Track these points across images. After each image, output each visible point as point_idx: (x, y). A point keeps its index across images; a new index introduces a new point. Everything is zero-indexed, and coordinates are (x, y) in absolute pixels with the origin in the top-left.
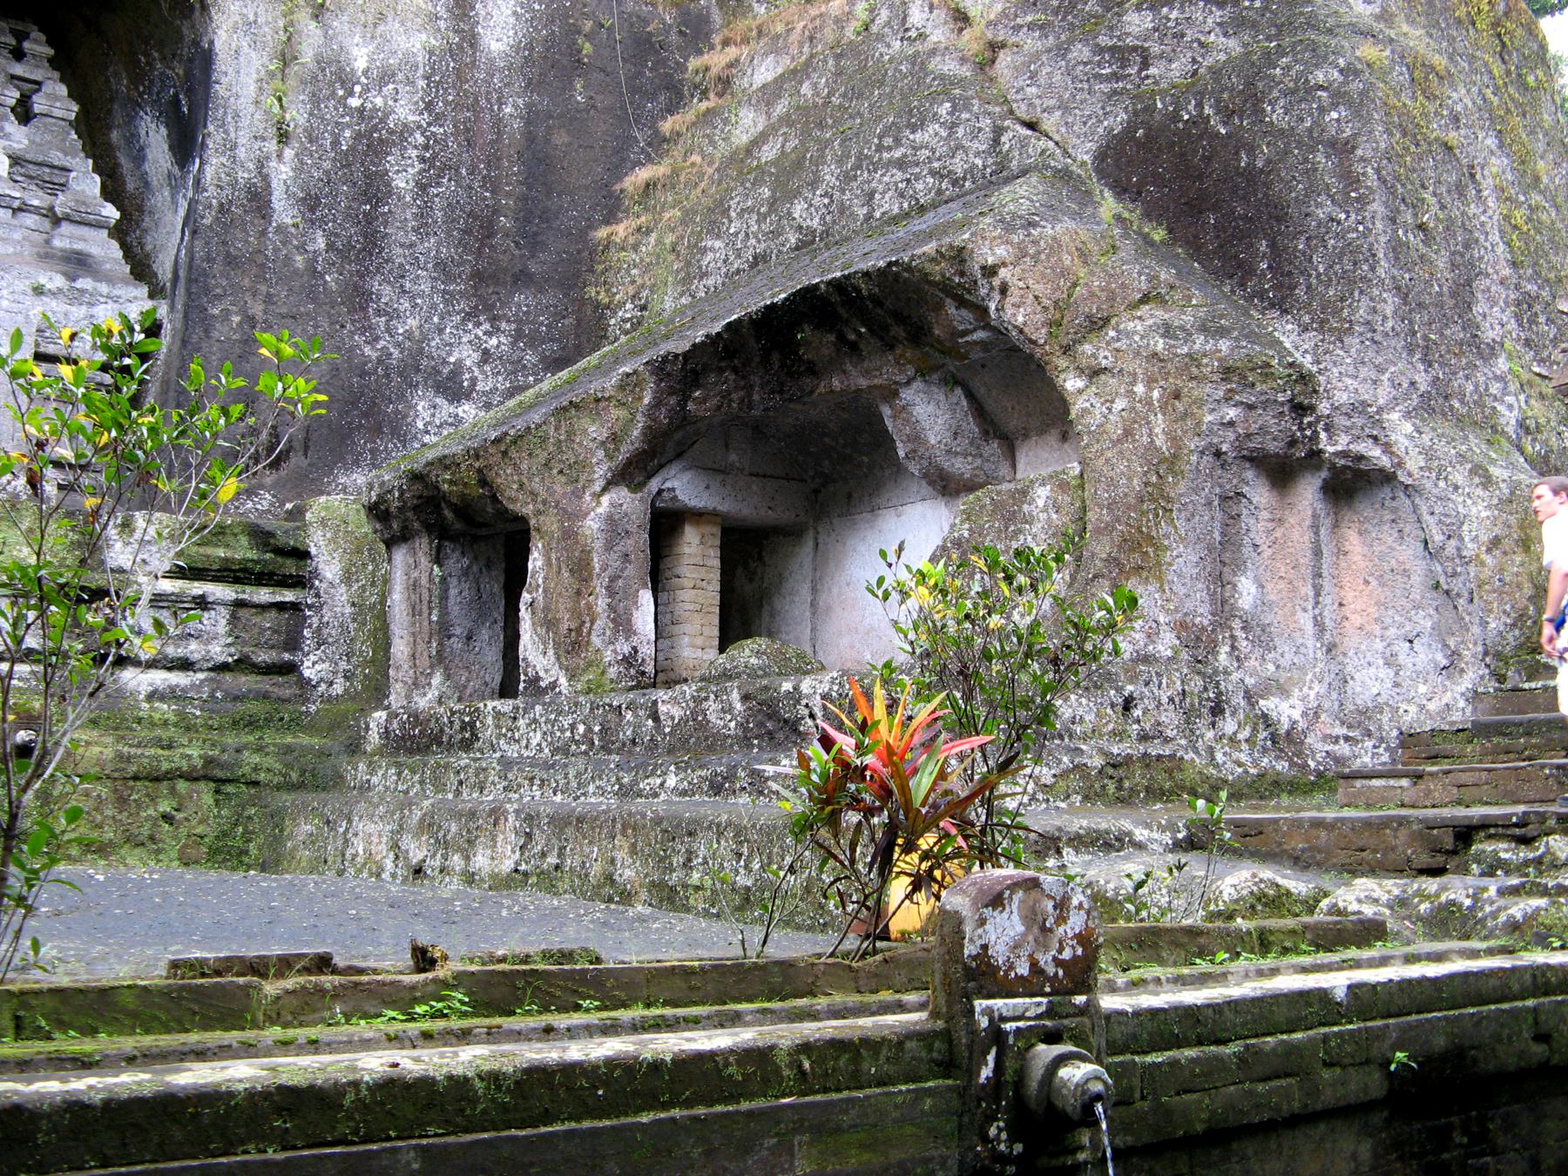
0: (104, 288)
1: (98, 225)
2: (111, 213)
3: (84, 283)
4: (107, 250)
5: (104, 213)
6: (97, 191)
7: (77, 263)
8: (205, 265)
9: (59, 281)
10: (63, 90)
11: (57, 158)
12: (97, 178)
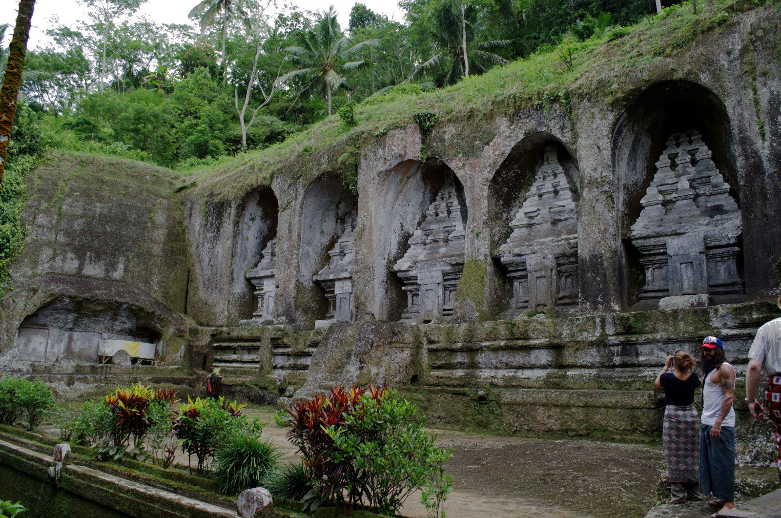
0: (725, 216)
1: (724, 193)
2: (727, 186)
3: (718, 217)
4: (727, 202)
5: (723, 187)
6: (722, 180)
7: (718, 210)
8: (745, 200)
9: (708, 219)
10: (706, 148)
11: (705, 174)
12: (721, 175)
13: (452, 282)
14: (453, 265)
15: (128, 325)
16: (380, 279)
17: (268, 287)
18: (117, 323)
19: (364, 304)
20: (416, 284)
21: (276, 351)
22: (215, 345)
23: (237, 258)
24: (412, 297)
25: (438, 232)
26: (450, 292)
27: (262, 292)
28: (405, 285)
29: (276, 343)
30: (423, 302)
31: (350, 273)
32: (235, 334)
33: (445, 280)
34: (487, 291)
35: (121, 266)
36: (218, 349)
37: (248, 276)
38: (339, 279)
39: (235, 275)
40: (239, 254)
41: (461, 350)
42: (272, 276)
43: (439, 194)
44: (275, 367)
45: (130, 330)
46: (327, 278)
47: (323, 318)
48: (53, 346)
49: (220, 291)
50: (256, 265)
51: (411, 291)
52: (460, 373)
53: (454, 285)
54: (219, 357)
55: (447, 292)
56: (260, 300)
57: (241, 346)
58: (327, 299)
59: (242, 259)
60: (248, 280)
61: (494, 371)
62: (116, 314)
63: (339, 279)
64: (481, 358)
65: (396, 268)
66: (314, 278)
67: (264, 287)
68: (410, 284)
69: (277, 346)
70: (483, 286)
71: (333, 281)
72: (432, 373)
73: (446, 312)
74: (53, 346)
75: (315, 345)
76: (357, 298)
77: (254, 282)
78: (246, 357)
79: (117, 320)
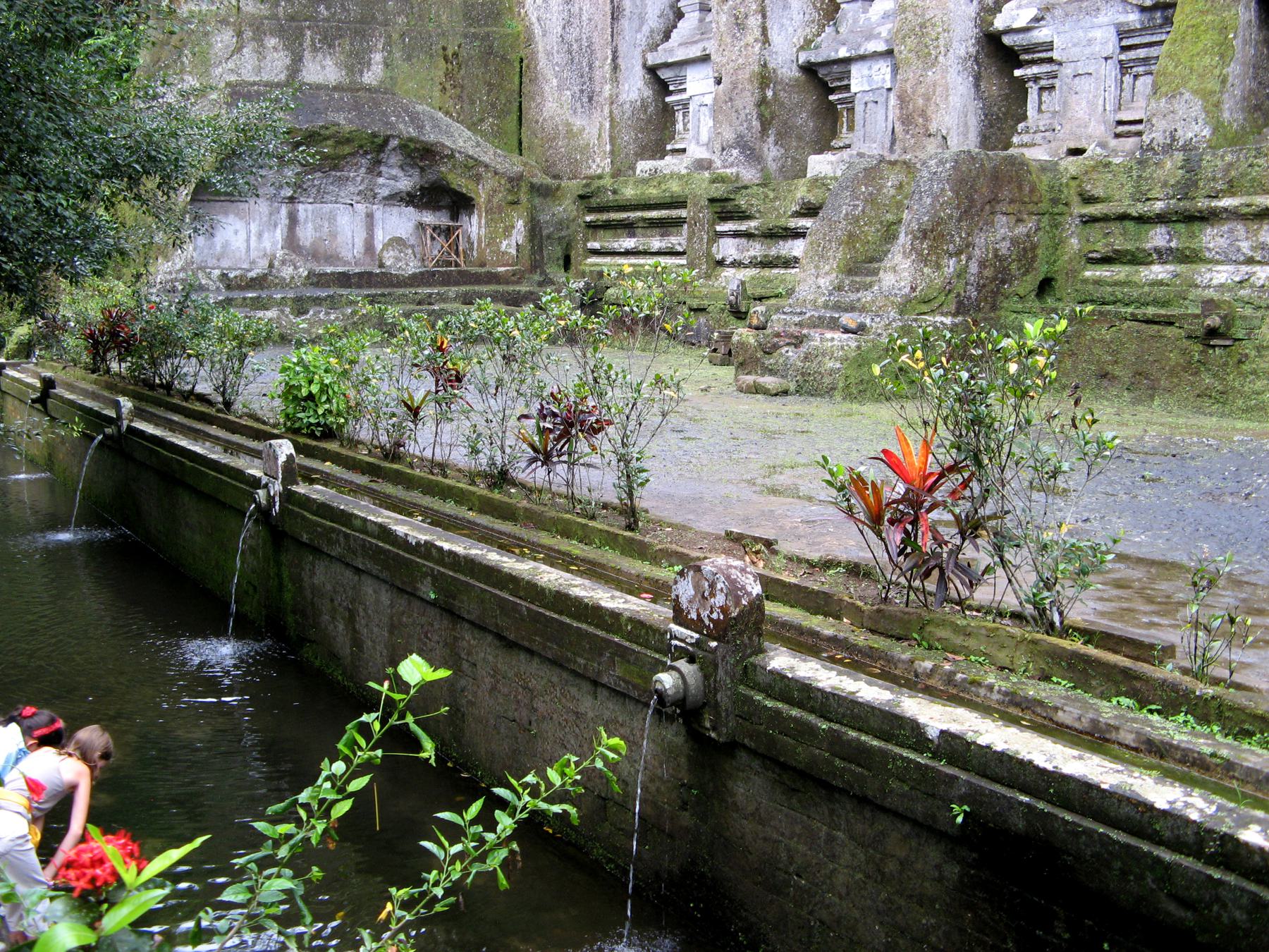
13: (1142, 53)
14: (1143, 9)
15: (405, 183)
16: (962, 52)
17: (698, 84)
18: (381, 180)
19: (923, 114)
20: (1050, 60)
21: (719, 228)
22: (588, 219)
23: (624, 23)
26: (1136, 77)
27: (684, 96)
28: (1020, 65)
29: (725, 209)
30: (1065, 104)
31: (887, 41)
32: (629, 192)
33: (1125, 49)
34: (1234, 70)
35: (377, 57)
36: (592, 226)
37: (652, 59)
38: (862, 58)
39: (620, 61)
40: (627, 13)
41: (1161, 219)
42: (705, 59)
44: (721, 263)
45: (409, 194)
46: (833, 56)
47: (823, 146)
48: (260, 235)
49: (590, 99)
50: (667, 36)
51: (1036, 79)
52: (1159, 271)
53: (1145, 61)
54: (596, 245)
55: (1128, 79)
56: (679, 116)
57: (644, 220)
58: (832, 105)
59: (635, 24)
60: (652, 70)
61: (1244, 269)
62: (378, 162)
63: (862, 58)
64: (1211, 238)
65: (1000, 23)
66: (803, 58)
67: (688, 85)
69: (725, 217)
70: (1224, 55)
71: (847, 61)
72: (1088, 274)
73: (1126, 128)
74: (260, 235)
75: (810, 211)
76: (903, 100)
77: (664, 74)
78: (656, 244)
79: (380, 174)
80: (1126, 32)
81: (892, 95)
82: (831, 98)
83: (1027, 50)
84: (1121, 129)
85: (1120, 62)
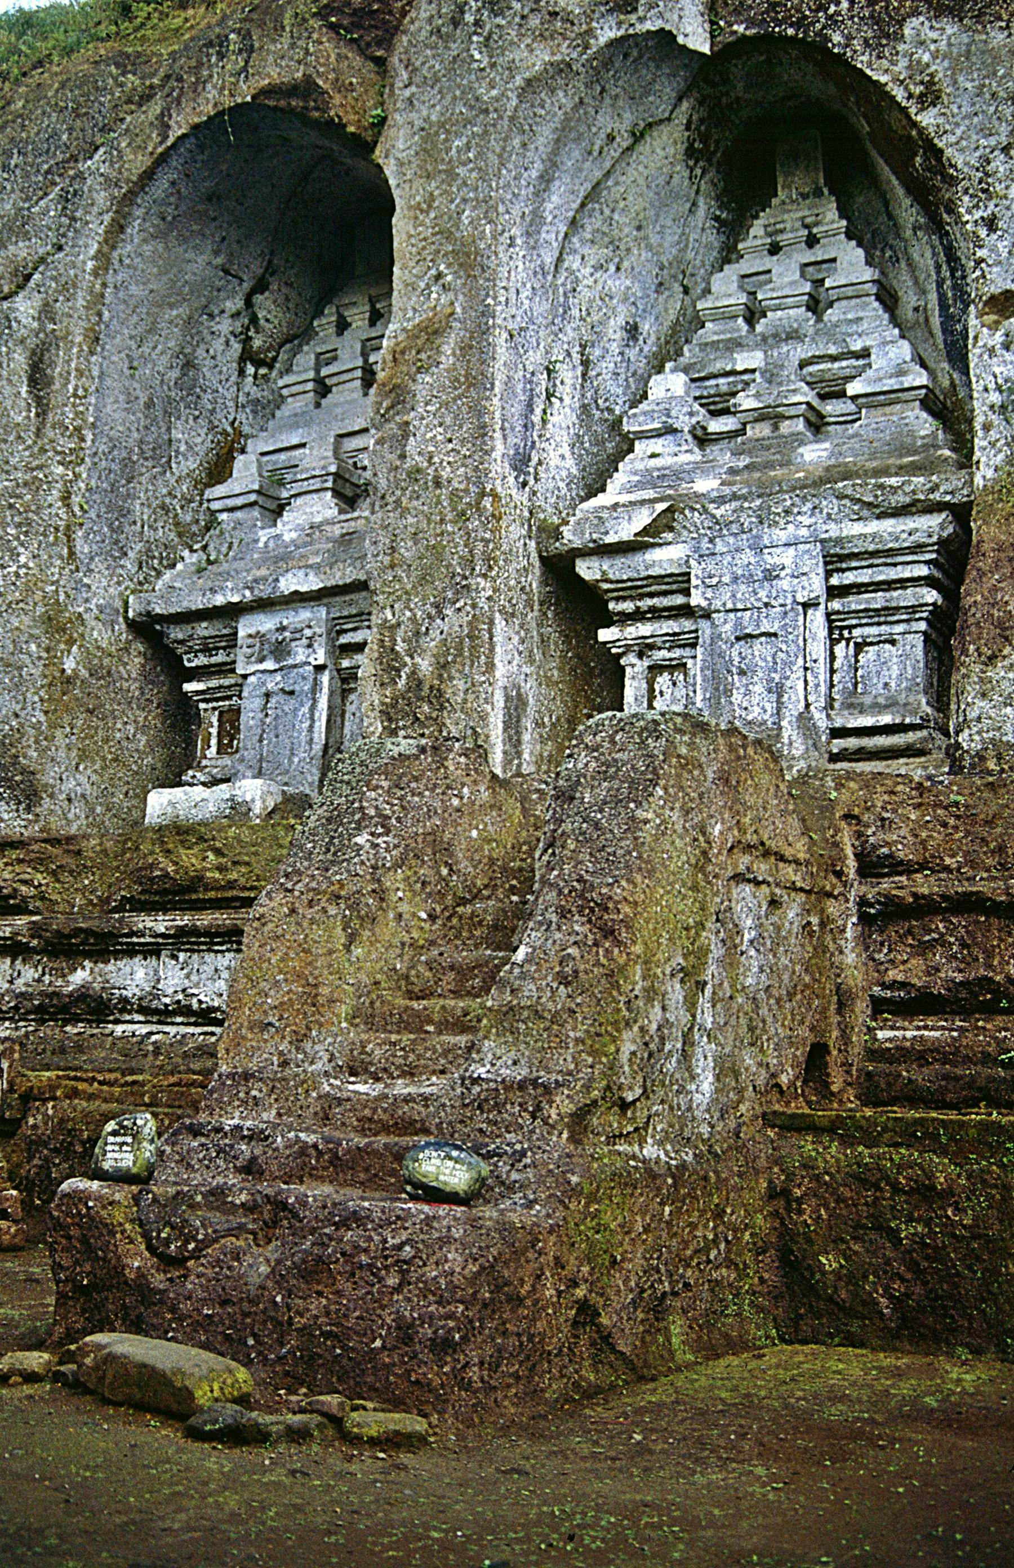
20: (686, 611)
24: (651, 684)
25: (771, 375)
26: (859, 647)
33: (834, 592)
43: (757, 229)
51: (644, 648)
68: (638, 616)
80: (842, 558)
81: (325, 678)
82: (189, 687)
83: (633, 589)
84: (838, 744)
85: (828, 615)
